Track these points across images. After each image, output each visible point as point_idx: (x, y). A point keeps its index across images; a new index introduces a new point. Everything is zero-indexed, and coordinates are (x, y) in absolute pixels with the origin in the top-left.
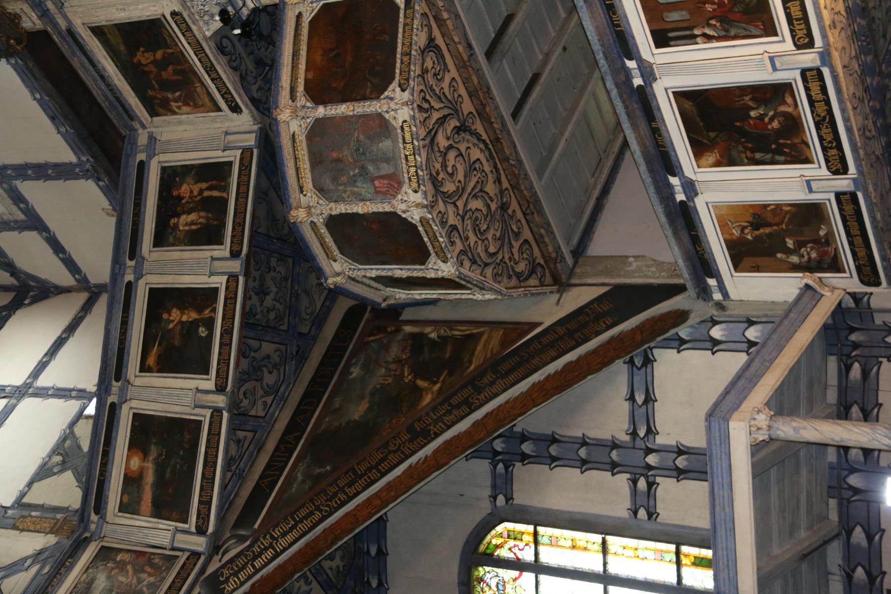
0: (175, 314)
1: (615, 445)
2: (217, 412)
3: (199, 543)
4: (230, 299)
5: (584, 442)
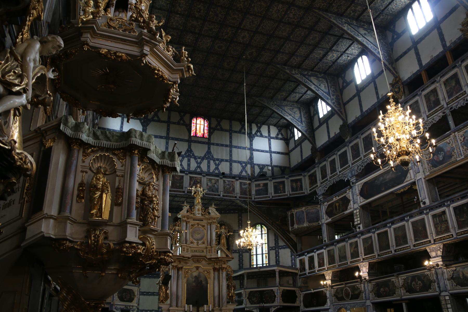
0: (281, 186)
1: (278, 244)
2: (269, 197)
3: (253, 199)
4: (284, 195)
5: (278, 239)
